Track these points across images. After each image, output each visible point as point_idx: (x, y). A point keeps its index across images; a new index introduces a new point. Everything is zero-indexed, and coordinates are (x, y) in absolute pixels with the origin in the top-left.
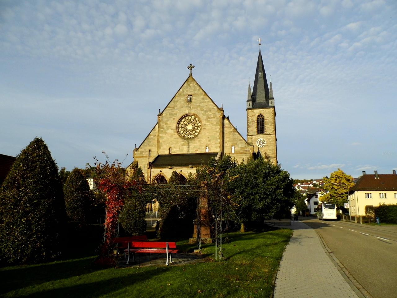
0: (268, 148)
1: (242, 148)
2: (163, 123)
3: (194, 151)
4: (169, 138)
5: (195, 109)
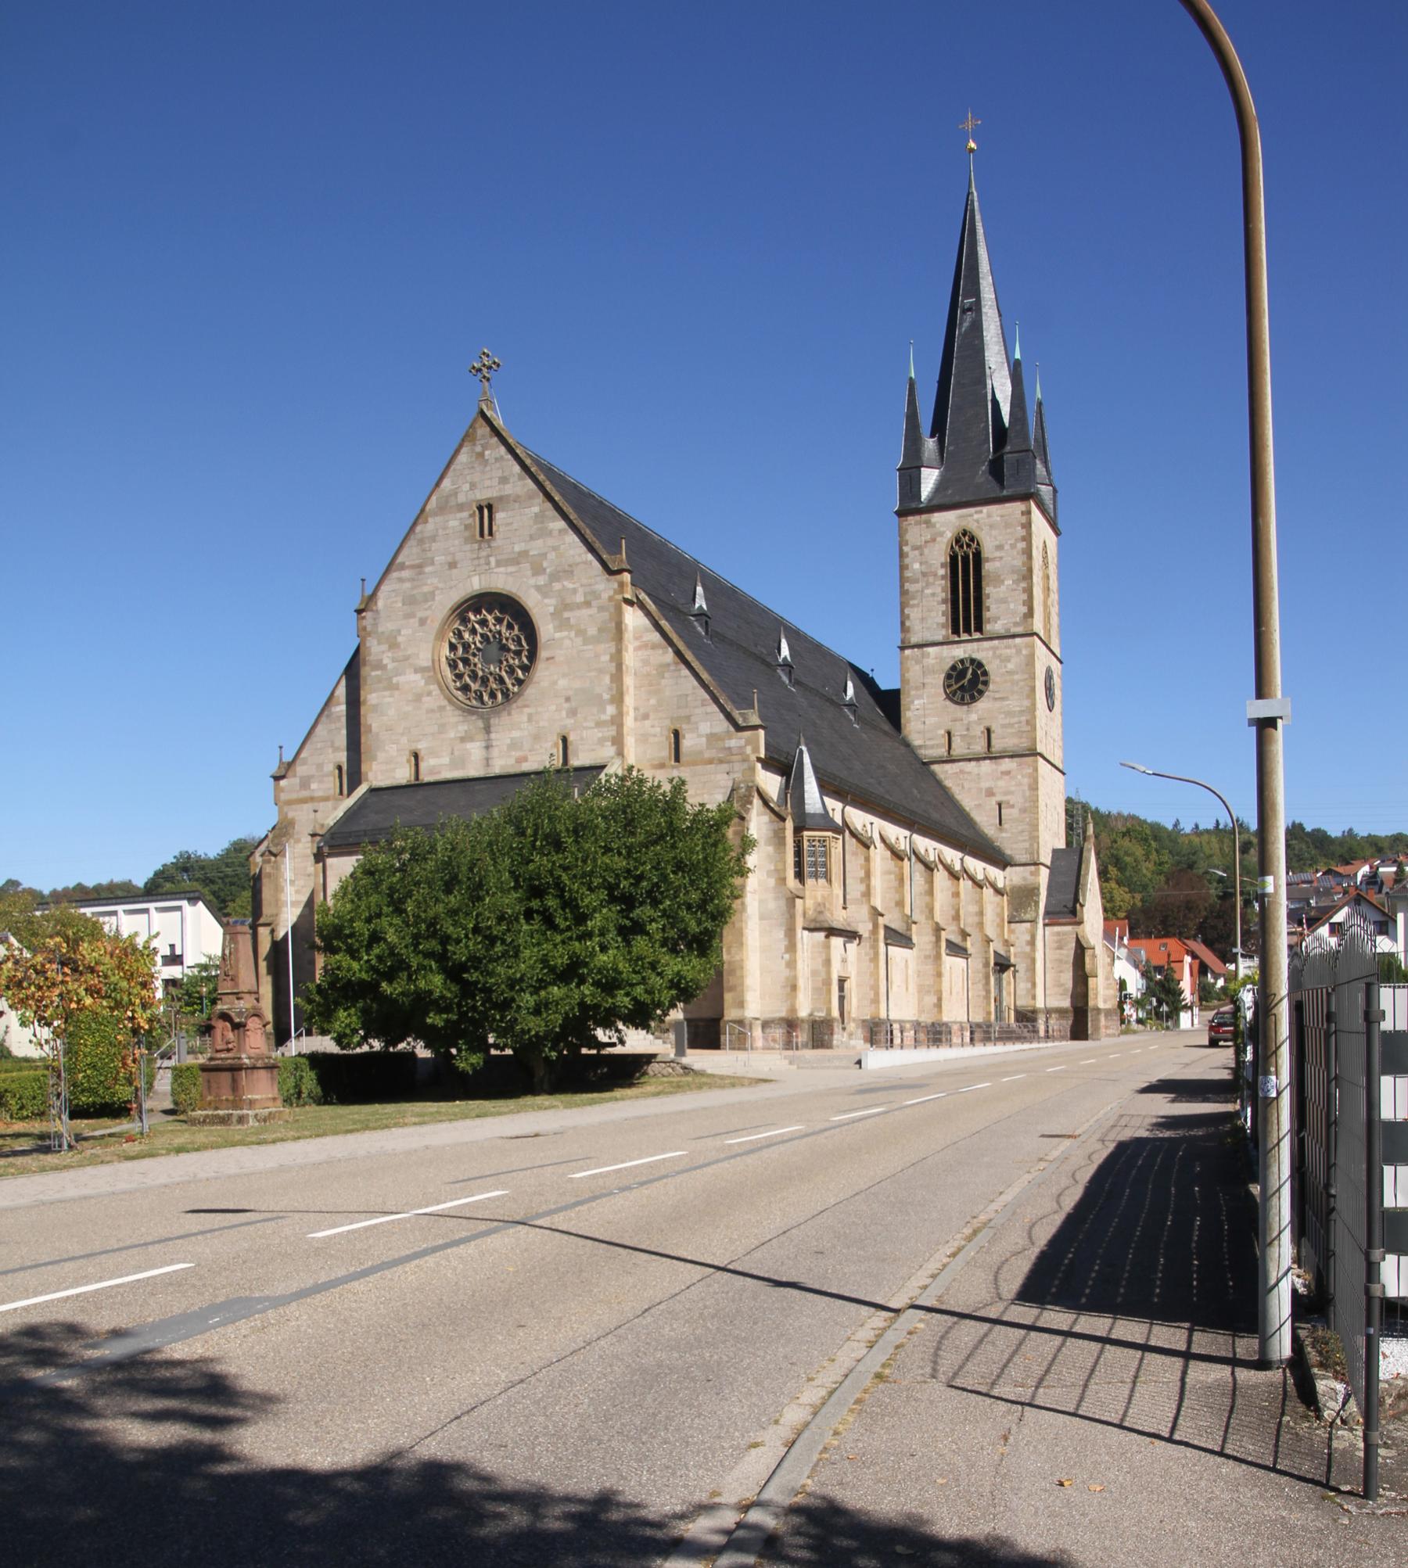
0: (998, 704)
1: (712, 738)
3: (512, 761)
4: (410, 708)
5: (511, 569)
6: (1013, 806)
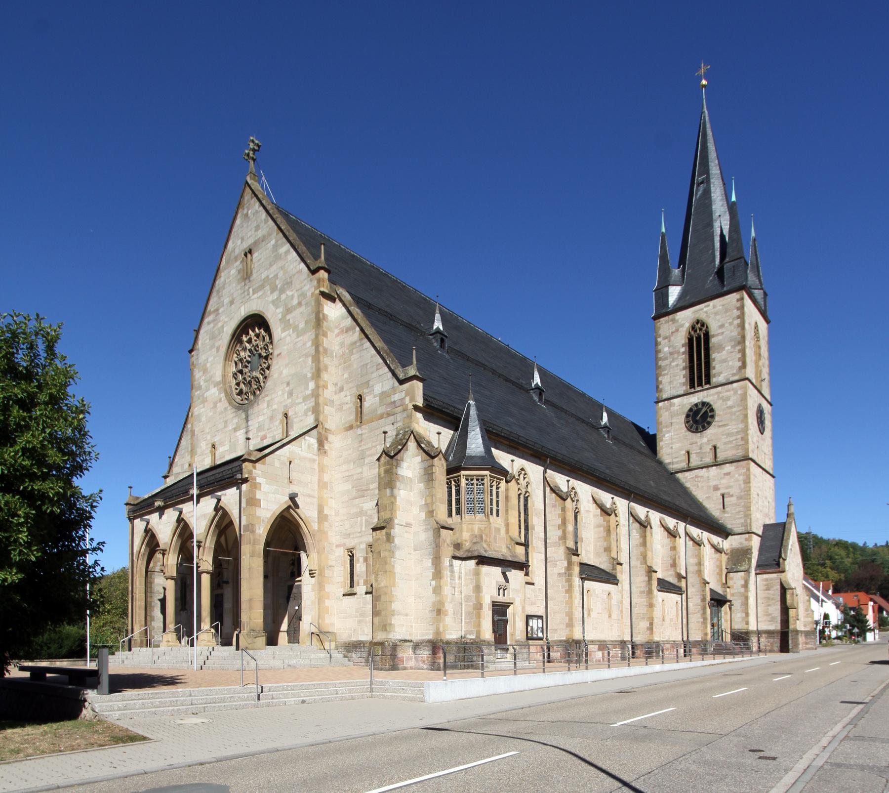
0: (721, 430)
6: (732, 496)
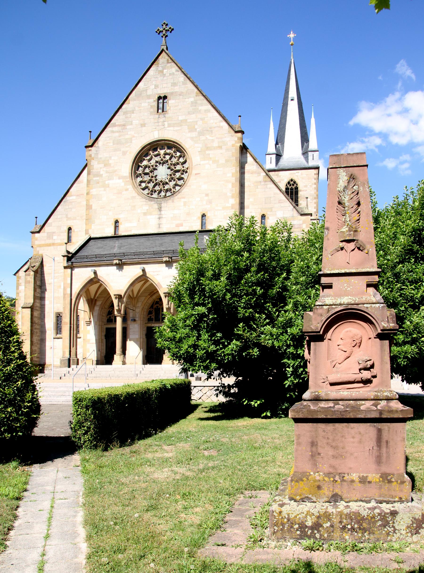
2: (98, 164)
5: (176, 128)
